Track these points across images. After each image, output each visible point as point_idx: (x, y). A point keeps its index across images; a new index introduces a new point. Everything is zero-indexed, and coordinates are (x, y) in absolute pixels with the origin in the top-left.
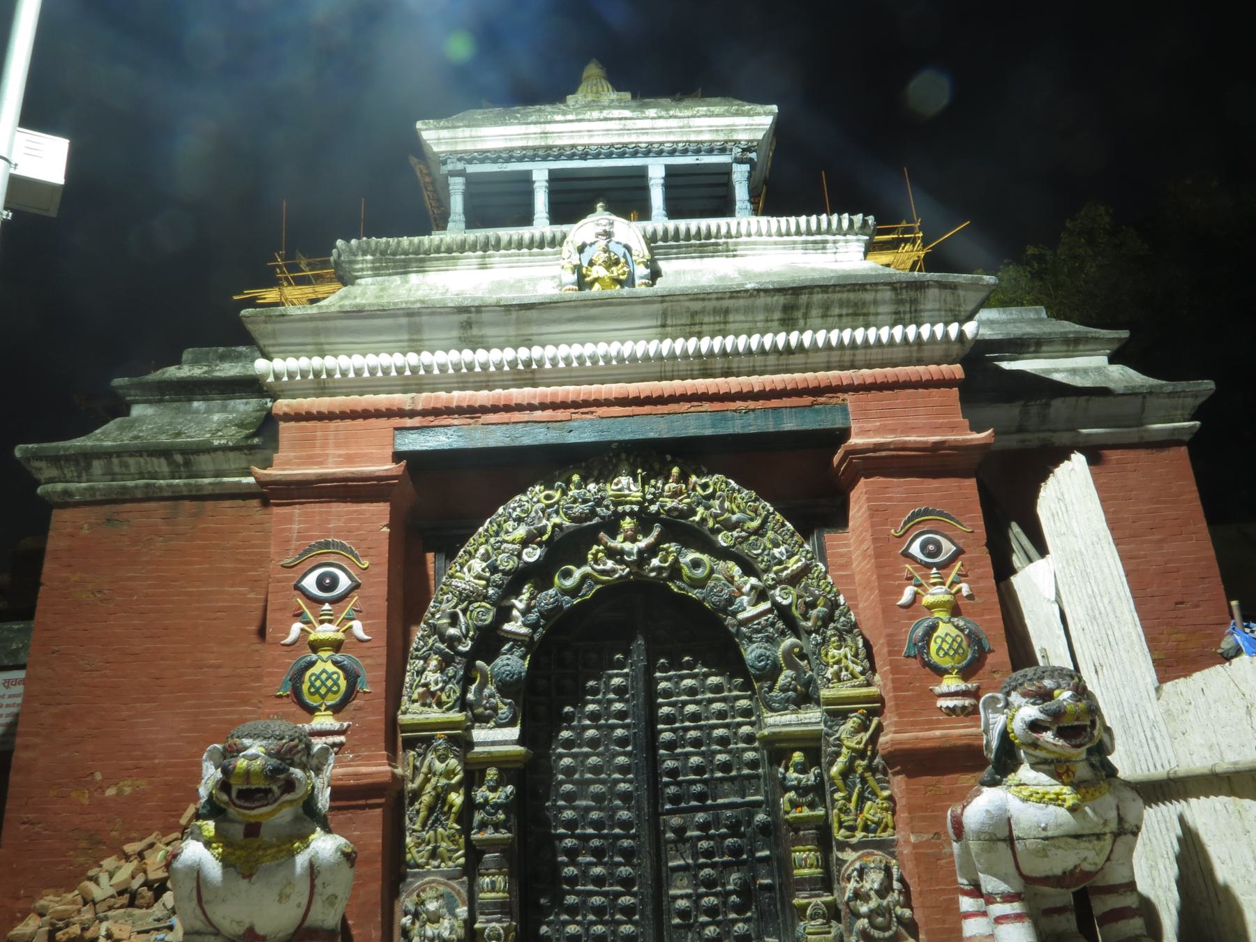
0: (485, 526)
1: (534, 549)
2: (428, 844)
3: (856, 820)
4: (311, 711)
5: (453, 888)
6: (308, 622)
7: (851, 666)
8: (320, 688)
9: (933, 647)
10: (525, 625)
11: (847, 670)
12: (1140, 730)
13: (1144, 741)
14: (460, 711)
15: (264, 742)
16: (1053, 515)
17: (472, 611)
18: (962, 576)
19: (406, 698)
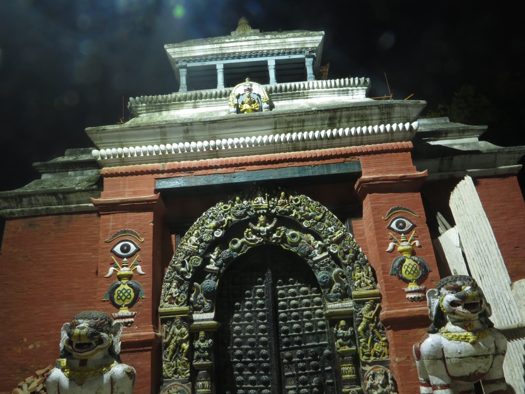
0: (197, 221)
1: (219, 231)
2: (173, 367)
3: (370, 352)
4: (118, 307)
5: (184, 388)
6: (117, 267)
7: (366, 280)
8: (122, 296)
9: (404, 270)
10: (216, 266)
11: (364, 282)
12: (503, 305)
13: (505, 310)
14: (187, 306)
15: (88, 321)
16: (457, 206)
17: (191, 260)
18: (416, 237)
19: (162, 300)
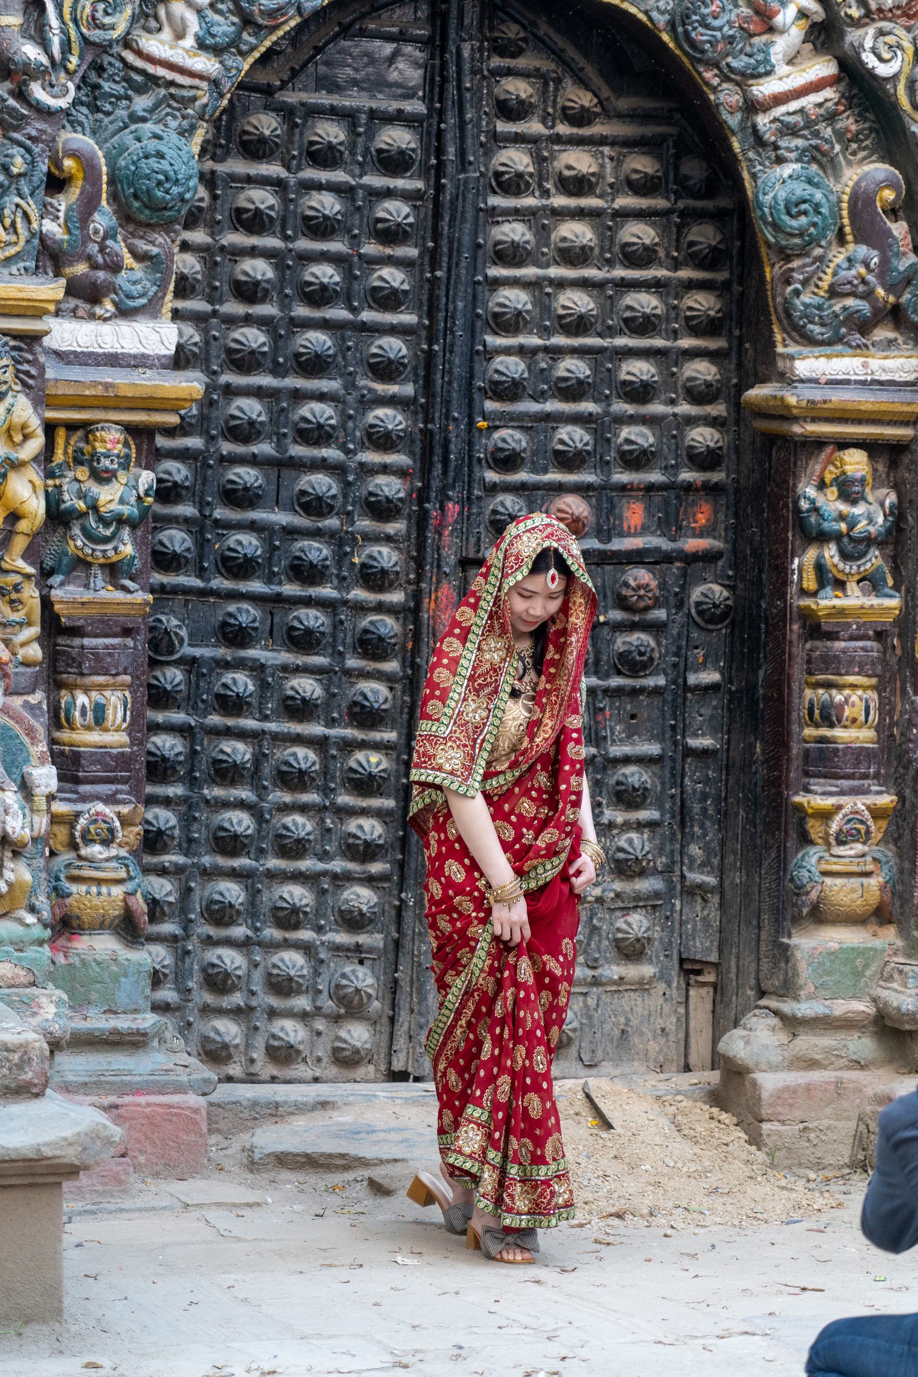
10: (202, 45)
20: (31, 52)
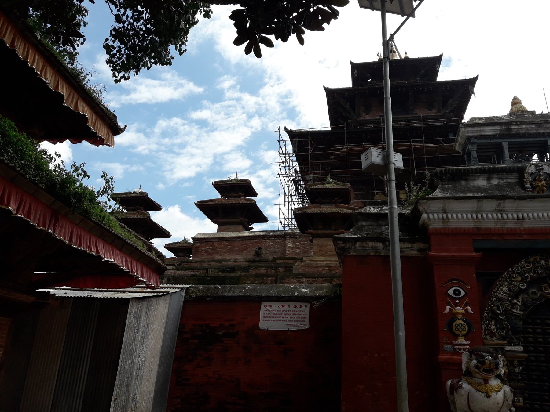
1: (524, 284)
4: (456, 337)
10: (520, 310)
20: (498, 311)
